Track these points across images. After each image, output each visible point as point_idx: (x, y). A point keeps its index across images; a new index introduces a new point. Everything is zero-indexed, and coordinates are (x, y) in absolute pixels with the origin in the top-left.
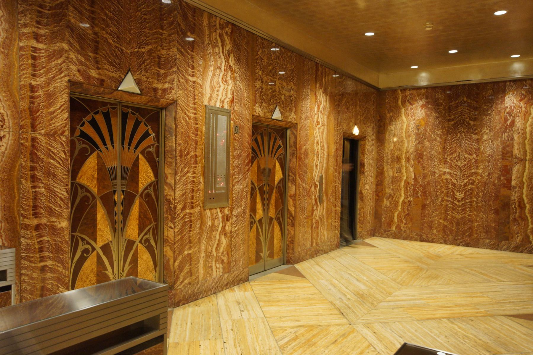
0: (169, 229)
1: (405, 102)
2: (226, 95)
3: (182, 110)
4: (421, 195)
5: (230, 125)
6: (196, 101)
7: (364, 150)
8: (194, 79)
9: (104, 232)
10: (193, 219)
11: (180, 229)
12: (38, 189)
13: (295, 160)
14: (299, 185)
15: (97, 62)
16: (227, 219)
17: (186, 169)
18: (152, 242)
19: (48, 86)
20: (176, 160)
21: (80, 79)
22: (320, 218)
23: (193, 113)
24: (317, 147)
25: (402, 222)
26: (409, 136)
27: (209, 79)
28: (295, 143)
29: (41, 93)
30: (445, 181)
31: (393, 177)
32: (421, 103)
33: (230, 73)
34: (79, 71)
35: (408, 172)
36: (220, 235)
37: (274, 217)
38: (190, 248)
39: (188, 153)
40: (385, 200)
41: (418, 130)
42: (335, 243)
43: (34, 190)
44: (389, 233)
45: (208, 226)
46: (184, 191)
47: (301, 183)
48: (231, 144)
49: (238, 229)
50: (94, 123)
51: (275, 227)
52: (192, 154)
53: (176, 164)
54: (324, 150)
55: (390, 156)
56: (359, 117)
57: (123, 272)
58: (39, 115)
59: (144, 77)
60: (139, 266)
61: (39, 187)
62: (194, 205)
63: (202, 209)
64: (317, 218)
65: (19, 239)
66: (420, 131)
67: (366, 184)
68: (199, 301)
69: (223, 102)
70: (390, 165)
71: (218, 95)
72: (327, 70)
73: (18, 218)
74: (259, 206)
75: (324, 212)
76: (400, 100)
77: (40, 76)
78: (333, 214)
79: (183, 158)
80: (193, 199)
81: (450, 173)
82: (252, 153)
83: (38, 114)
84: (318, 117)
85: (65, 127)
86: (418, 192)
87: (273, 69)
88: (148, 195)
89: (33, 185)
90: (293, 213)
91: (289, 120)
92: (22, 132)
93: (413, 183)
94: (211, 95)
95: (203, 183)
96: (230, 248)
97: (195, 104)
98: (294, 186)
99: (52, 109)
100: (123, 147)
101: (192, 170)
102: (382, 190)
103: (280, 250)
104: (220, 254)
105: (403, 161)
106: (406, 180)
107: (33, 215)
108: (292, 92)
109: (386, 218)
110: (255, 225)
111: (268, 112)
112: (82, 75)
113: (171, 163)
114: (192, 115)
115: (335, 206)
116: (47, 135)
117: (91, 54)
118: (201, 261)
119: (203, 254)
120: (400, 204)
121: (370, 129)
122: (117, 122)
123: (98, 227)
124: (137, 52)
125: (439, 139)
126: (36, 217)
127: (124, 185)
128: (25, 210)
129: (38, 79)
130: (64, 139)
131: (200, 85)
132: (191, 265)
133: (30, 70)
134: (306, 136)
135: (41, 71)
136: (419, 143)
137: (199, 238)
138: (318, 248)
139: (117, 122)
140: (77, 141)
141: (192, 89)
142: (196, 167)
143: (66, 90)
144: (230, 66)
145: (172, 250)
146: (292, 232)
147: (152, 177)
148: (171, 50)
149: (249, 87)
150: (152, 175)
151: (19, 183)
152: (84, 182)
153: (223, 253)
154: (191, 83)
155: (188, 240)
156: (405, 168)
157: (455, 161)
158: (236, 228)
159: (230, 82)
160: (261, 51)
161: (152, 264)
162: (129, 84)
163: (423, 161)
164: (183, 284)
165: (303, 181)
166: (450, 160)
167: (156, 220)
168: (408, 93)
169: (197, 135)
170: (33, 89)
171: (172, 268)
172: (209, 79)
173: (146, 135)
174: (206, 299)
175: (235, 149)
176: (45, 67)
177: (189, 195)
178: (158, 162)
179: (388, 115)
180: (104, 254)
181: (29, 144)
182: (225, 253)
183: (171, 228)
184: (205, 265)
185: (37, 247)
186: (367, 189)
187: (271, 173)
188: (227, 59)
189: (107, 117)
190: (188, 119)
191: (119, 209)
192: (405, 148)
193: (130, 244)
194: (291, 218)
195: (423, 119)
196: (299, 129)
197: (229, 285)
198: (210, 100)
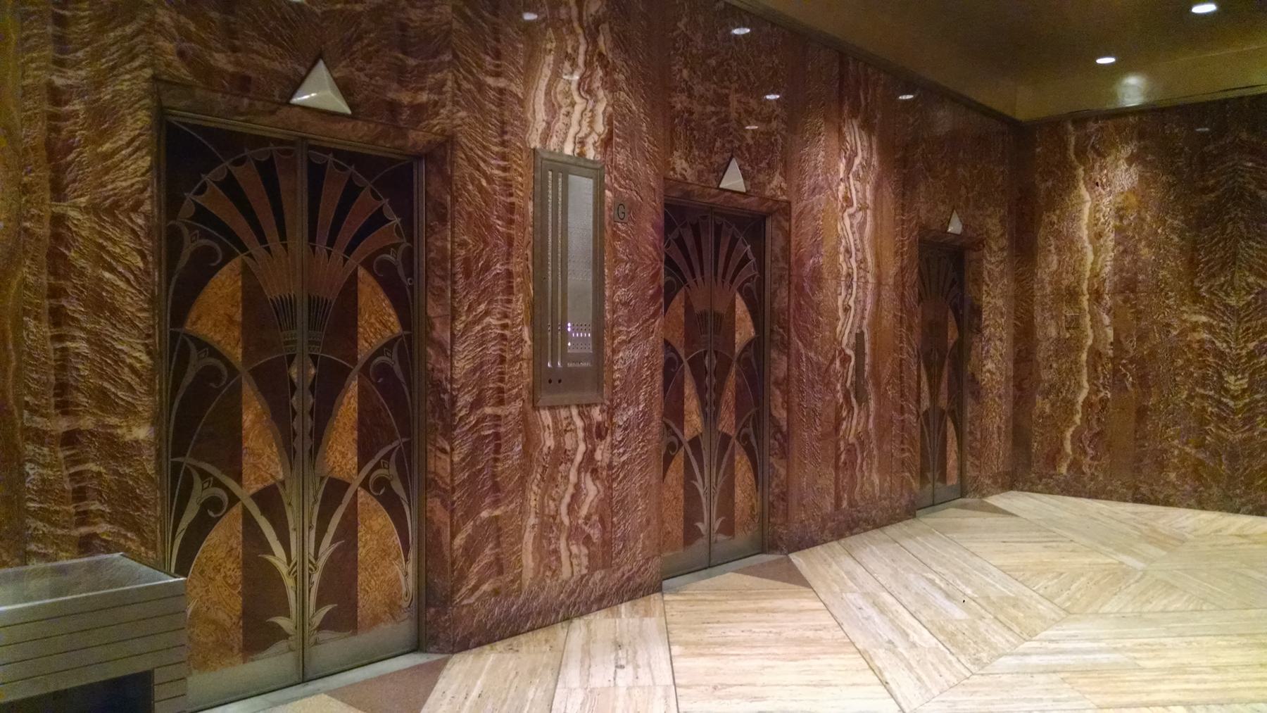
0: (439, 454)
1: (1084, 152)
2: (591, 124)
3: (469, 159)
4: (1133, 385)
5: (602, 202)
6: (506, 138)
7: (981, 273)
8: (502, 83)
9: (263, 460)
10: (502, 430)
11: (467, 455)
12: (69, 344)
13: (785, 294)
14: (799, 355)
15: (232, 34)
16: (597, 433)
17: (483, 307)
18: (397, 487)
19: (96, 88)
20: (454, 283)
21: (184, 72)
22: (858, 438)
23: (499, 167)
24: (847, 261)
25: (1085, 453)
26: (1099, 235)
27: (543, 85)
28: (786, 250)
29: (77, 107)
30: (1196, 346)
31: (1058, 339)
32: (1127, 151)
33: (600, 73)
34: (181, 54)
35: (1099, 329)
36: (579, 473)
37: (733, 433)
38: (496, 504)
39: (487, 267)
40: (1039, 398)
41: (1121, 218)
42: (904, 502)
43: (58, 346)
44: (1052, 483)
45: (545, 450)
46: (478, 361)
47: (803, 351)
48: (607, 248)
49: (630, 461)
50: (231, 187)
51: (737, 458)
52: (499, 268)
53: (454, 291)
54: (865, 270)
55: (1049, 289)
56: (963, 191)
57: (316, 558)
58: (73, 161)
59: (361, 74)
60: (360, 544)
61: (73, 339)
62: (506, 396)
63: (529, 407)
64: (852, 439)
65: (22, 465)
66: (1125, 222)
67: (986, 358)
68: (522, 638)
69: (582, 143)
70: (1050, 310)
71: (568, 126)
72: (870, 70)
73: (16, 413)
74: (692, 405)
75: (871, 425)
76: (1072, 148)
77: (77, 65)
78: (895, 430)
79: (473, 279)
80: (502, 380)
81: (1209, 327)
82: (668, 273)
83: (69, 158)
84: (848, 188)
85: (143, 191)
86: (1125, 375)
87: (720, 64)
88: (385, 370)
89: (56, 332)
90: (784, 424)
91: (768, 193)
92: (27, 201)
93: (1111, 352)
94: (548, 124)
95: (529, 342)
96: (608, 509)
97: (503, 144)
98: (785, 358)
99: (107, 147)
100: (313, 248)
101: (498, 308)
102: (1031, 374)
103: (753, 517)
104: (580, 521)
105: (1085, 301)
106: (1091, 347)
107: (57, 407)
108: (774, 124)
109: (1041, 443)
110: (681, 453)
111: (709, 172)
112: (189, 65)
113: (443, 290)
114: (496, 172)
115: (902, 411)
116: (93, 209)
117: (214, 15)
118: (529, 537)
119: (532, 520)
120: (1079, 407)
121: (996, 221)
122: (294, 188)
123: (246, 445)
124: (341, 12)
125: (1176, 239)
126: (65, 413)
127: (317, 343)
128: (35, 394)
129: (70, 73)
130: (140, 221)
131: (519, 98)
132: (498, 545)
133: (49, 51)
134: (815, 234)
135: (80, 54)
136: (1125, 251)
137: (522, 478)
138: (855, 514)
139: (294, 188)
140: (185, 231)
141: (494, 108)
142: (509, 301)
143: (147, 101)
144: (600, 54)
145: (445, 507)
146: (783, 472)
147: (395, 327)
148: (436, 9)
149: (653, 107)
150: (393, 319)
151: (19, 325)
152: (205, 332)
153: (588, 518)
154: (491, 93)
155: (489, 483)
156: (1088, 317)
157: (1222, 294)
158: (624, 458)
159: (601, 93)
160: (685, 20)
161: (398, 541)
162: (318, 92)
163: (1137, 299)
164: (477, 594)
165: (809, 345)
166: (1208, 291)
167: (407, 432)
168: (1092, 127)
169: (511, 222)
170: (56, 96)
171: (447, 553)
172: (543, 85)
173: (377, 220)
174: (541, 635)
175: (618, 261)
176: (88, 44)
177: (492, 371)
178: (411, 288)
179: (1043, 186)
180: (264, 511)
181: (44, 230)
182: (595, 518)
183: (443, 451)
184: (538, 548)
185: (68, 486)
186: (989, 371)
187: (724, 324)
188: (592, 38)
189: (268, 171)
190: (484, 183)
191: (302, 401)
192: (1089, 267)
193: (335, 490)
194: (779, 436)
195: (1133, 191)
196: (794, 215)
197: (606, 600)
198: (546, 136)
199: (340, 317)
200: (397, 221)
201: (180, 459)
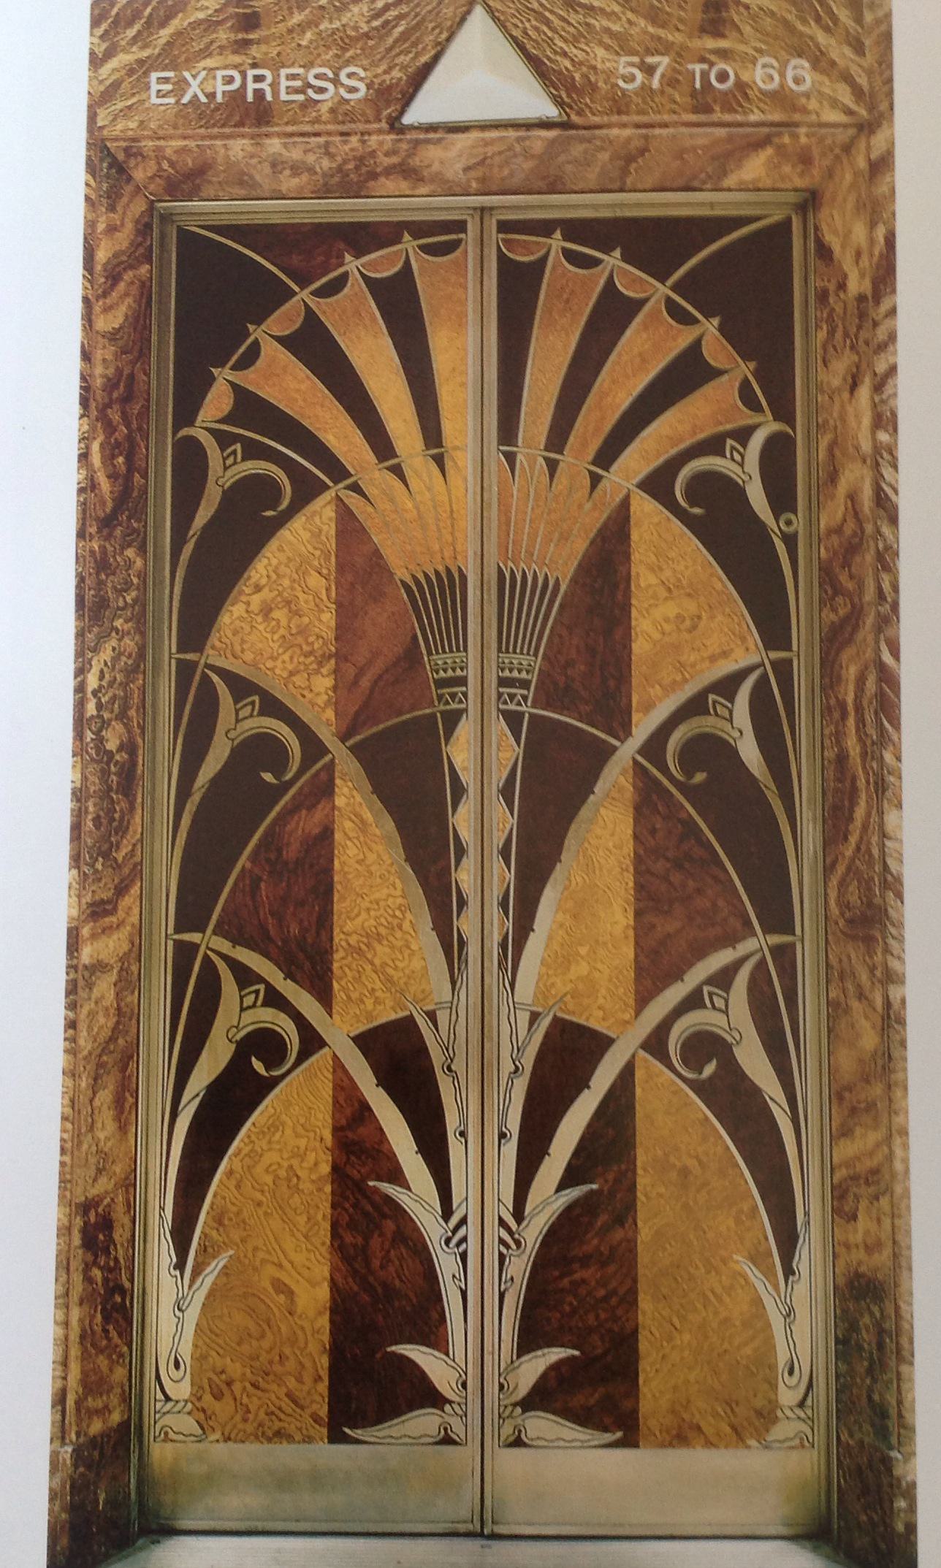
18: (754, 1062)
88: (712, 753)
100: (511, 458)
189: (401, 309)
200: (745, 369)
201: (195, 937)
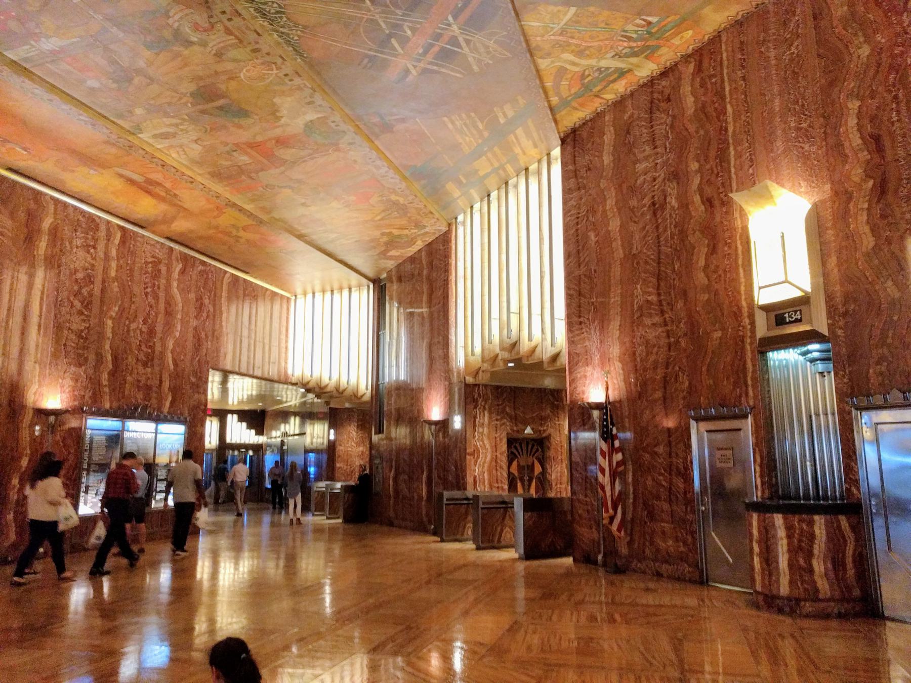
50: (516, 448)
122: (524, 446)
139: (524, 446)
173: (537, 450)
199: (531, 468)
